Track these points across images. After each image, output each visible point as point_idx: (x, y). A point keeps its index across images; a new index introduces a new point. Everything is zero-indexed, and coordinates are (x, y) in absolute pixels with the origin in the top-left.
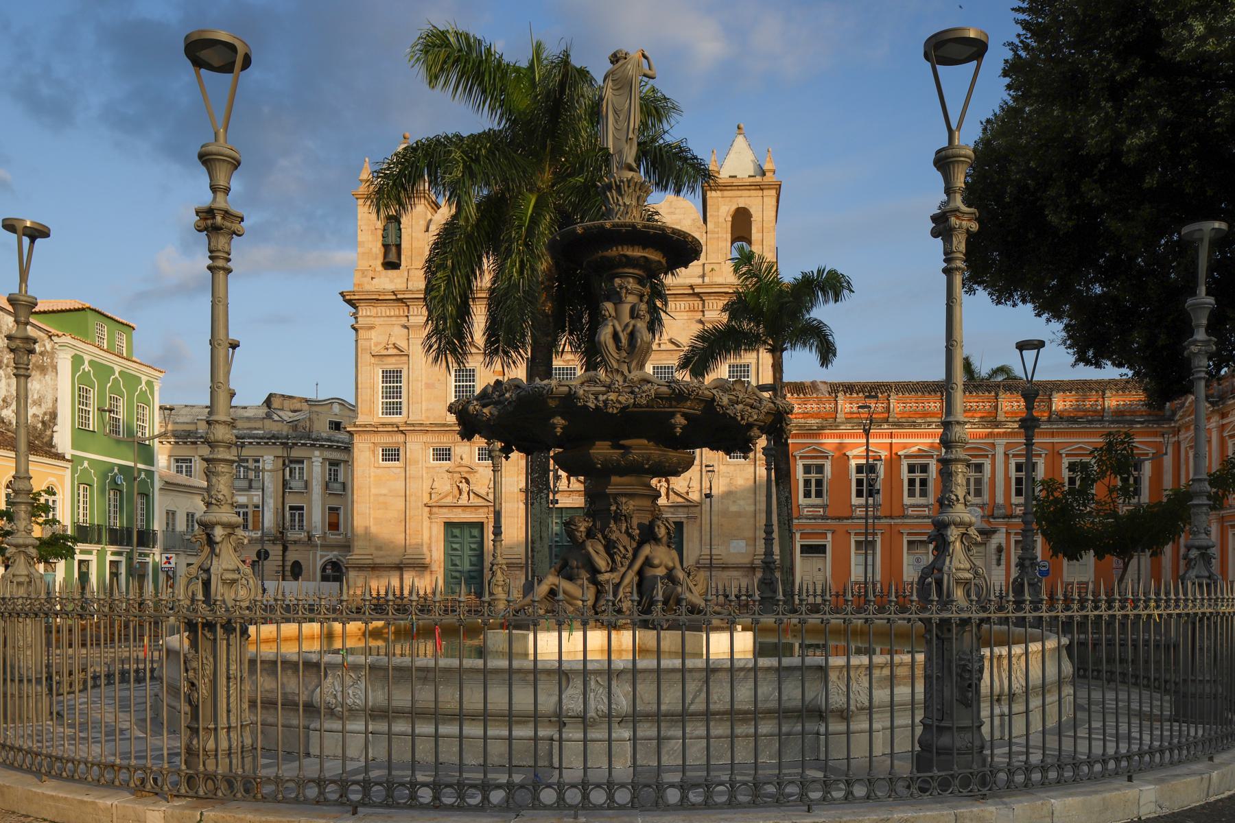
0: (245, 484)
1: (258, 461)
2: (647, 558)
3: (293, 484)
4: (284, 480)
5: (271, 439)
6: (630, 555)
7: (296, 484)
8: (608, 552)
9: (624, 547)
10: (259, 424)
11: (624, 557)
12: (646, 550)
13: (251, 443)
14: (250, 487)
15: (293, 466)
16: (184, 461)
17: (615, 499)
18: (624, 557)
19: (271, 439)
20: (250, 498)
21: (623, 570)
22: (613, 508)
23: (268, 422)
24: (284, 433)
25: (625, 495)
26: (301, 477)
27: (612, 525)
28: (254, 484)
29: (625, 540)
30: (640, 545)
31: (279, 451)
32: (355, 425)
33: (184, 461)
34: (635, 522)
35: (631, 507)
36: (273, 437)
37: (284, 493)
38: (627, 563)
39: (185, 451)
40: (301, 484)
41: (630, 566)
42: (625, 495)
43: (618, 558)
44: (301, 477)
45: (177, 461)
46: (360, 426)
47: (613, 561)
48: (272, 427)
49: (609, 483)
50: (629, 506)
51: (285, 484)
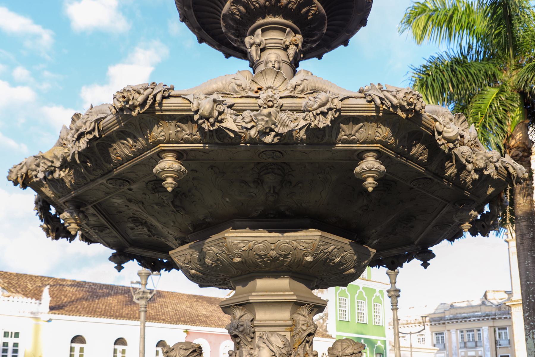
0: (473, 344)
1: (479, 330)
3: (501, 342)
4: (496, 340)
5: (486, 317)
7: (503, 342)
10: (478, 309)
13: (474, 320)
14: (476, 346)
15: (500, 331)
16: (440, 334)
19: (486, 317)
20: (477, 352)
23: (483, 307)
24: (493, 312)
26: (506, 338)
28: (478, 344)
31: (491, 323)
32: (512, 301)
33: (440, 334)
36: (487, 315)
37: (496, 348)
39: (439, 329)
40: (506, 342)
44: (506, 338)
45: (436, 334)
46: (515, 301)
48: (485, 310)
51: (496, 343)
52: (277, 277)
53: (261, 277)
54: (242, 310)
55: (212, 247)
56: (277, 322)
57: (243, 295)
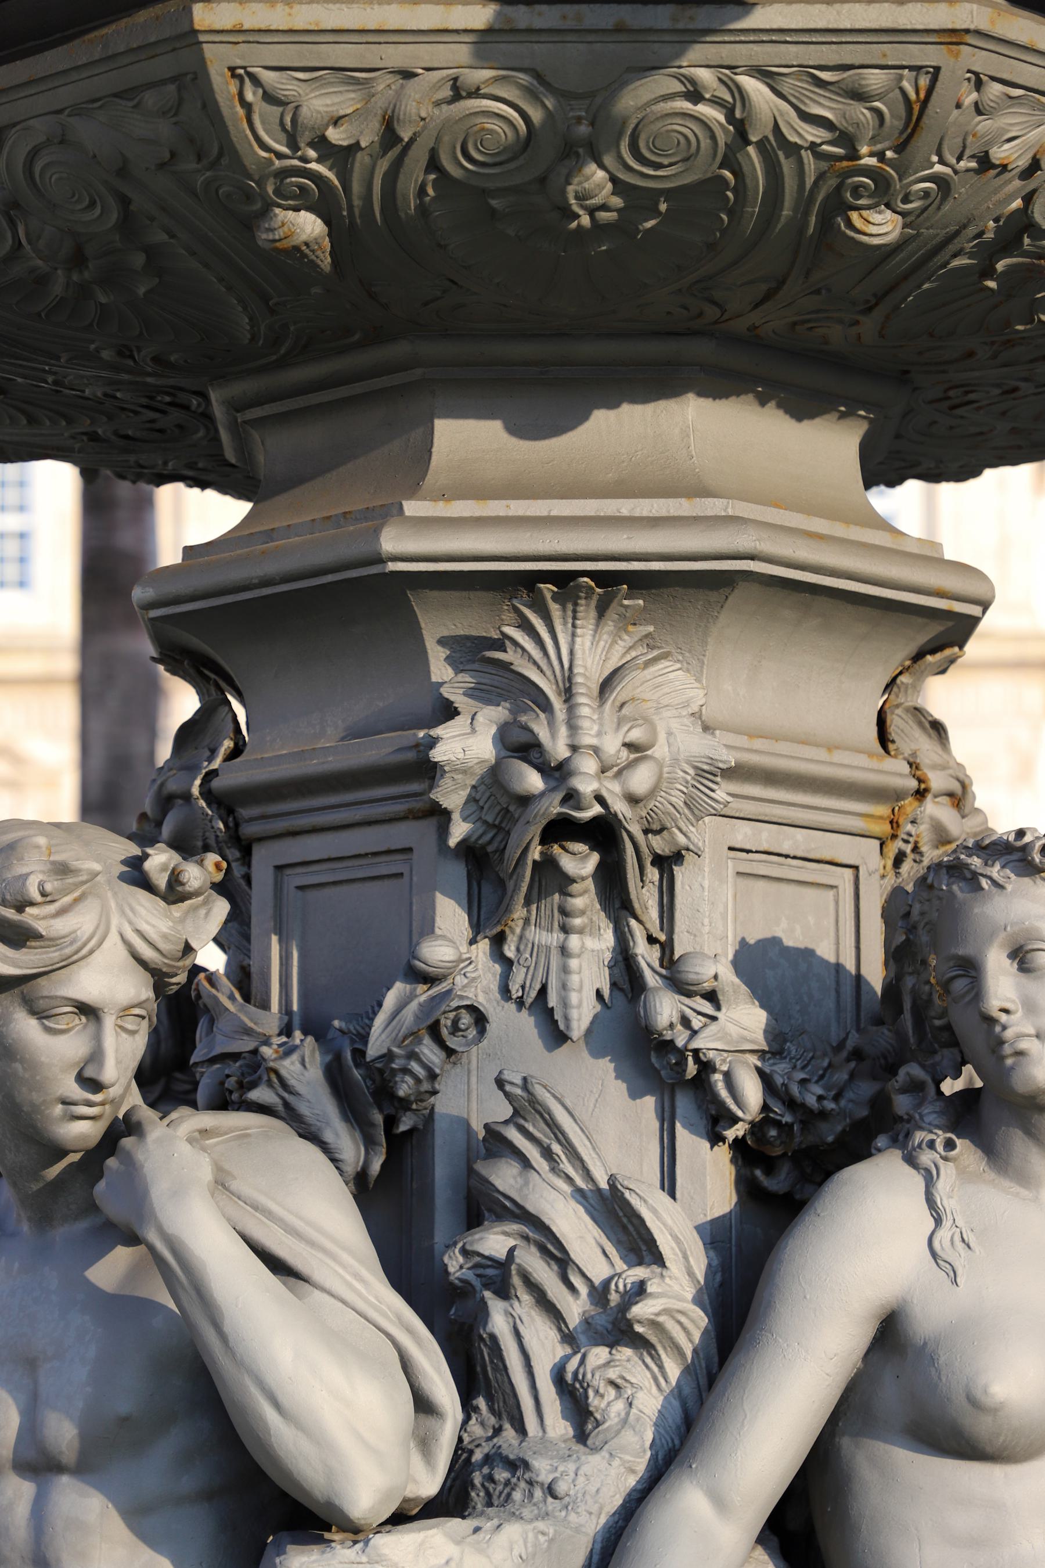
2: (890, 1335)
6: (675, 1297)
8: (409, 1269)
9: (614, 1212)
11: (615, 1326)
12: (878, 1238)
17: (470, 652)
18: (615, 1326)
21: (603, 1480)
22: (467, 744)
25: (613, 587)
27: (449, 936)
29: (612, 1124)
30: (786, 1177)
34: (715, 915)
35: (679, 743)
38: (639, 1394)
41: (681, 1444)
42: (613, 587)
43: (528, 1339)
47: (476, 1368)
49: (414, 469)
50: (648, 716)
52: (803, 405)
53: (720, 382)
54: (628, 621)
55: (751, 85)
56: (839, 757)
57: (625, 507)
